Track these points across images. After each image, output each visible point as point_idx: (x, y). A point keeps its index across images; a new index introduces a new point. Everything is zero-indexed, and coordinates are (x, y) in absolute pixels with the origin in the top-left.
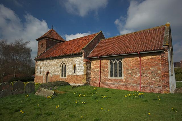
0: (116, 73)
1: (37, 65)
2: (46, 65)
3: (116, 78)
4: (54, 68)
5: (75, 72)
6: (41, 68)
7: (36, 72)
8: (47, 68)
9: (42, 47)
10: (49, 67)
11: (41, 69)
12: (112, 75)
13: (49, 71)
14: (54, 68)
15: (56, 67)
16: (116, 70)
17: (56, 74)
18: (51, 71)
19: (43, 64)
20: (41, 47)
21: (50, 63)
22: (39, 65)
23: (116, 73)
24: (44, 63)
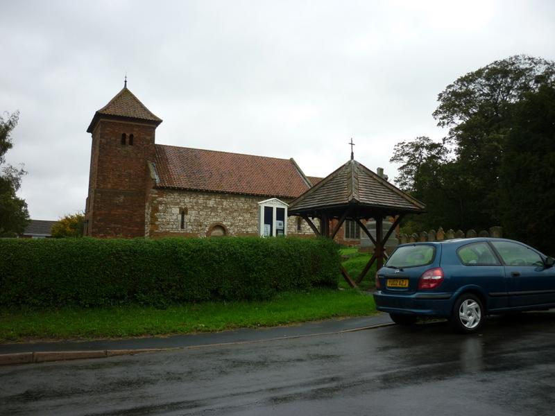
0: (353, 233)
1: (160, 203)
2: (206, 207)
3: (354, 240)
4: (240, 218)
5: (299, 228)
6: (184, 212)
7: (157, 223)
8: (213, 214)
9: (131, 143)
10: (223, 214)
11: (187, 217)
12: (347, 237)
13: (224, 223)
14: (240, 218)
15: (248, 216)
16: (353, 229)
17: (250, 230)
18: (229, 223)
19: (197, 203)
20: (123, 142)
21: (225, 203)
22: (178, 204)
23: (353, 233)
24: (201, 201)
